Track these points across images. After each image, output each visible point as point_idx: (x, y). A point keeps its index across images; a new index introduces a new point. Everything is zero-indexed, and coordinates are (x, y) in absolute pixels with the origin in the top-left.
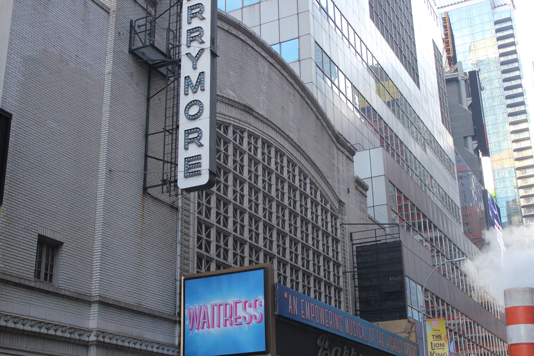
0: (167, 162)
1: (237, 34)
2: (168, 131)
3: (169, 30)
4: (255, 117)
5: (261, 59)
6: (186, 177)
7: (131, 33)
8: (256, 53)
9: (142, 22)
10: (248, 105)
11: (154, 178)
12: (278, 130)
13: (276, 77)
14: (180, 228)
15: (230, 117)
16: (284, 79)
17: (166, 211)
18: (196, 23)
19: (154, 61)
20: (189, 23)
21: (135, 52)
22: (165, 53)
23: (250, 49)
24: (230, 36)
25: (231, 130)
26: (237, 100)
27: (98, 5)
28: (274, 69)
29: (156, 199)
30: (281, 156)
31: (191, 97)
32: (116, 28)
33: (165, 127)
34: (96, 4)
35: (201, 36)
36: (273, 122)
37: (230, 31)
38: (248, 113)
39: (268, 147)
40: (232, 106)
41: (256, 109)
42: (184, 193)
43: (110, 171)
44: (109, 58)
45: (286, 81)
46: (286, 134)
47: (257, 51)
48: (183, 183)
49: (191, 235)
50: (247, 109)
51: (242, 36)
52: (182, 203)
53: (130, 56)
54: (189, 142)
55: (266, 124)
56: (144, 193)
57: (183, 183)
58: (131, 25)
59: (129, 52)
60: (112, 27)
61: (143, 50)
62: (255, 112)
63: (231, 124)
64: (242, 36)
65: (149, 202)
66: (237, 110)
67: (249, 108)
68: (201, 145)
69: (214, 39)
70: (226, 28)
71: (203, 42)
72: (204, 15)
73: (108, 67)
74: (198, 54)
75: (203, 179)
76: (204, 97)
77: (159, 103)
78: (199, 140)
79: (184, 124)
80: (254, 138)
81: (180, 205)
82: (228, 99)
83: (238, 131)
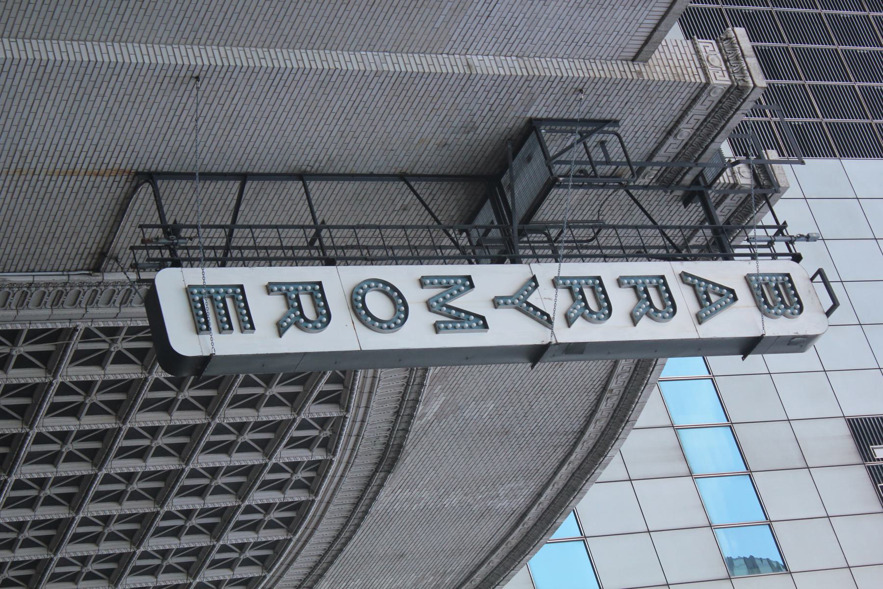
0: (230, 236)
1: (598, 415)
2: (317, 235)
3: (598, 226)
4: (371, 478)
5: (534, 486)
6: (189, 291)
7: (583, 122)
8: (550, 472)
9: (615, 151)
10: (402, 456)
11: (181, 204)
12: (337, 546)
13: (487, 532)
14: (41, 279)
15: (367, 408)
16: (482, 556)
17: (90, 238)
18: (622, 300)
19: (511, 188)
20: (620, 282)
21: (533, 136)
23: (560, 454)
24: (593, 397)
25: (330, 411)
26: (416, 424)
27: (655, 30)
28: (508, 525)
30: (262, 559)
31: (415, 297)
32: (595, 81)
33: (328, 227)
34: (658, 25)
35: (588, 315)
36: (359, 532)
37: (607, 395)
38: (381, 459)
39: (287, 521)
40: (397, 413)
41: (393, 481)
42: (145, 287)
43: (197, 78)
44: (510, 66)
45: (477, 561)
46: (326, 570)
47: (555, 474)
48: (171, 284)
49: (22, 313)
50: (390, 454)
51: (593, 431)
52: (115, 283)
53: (521, 123)
54: (289, 294)
55: (353, 512)
56: (137, 173)
57: (171, 284)
58: (606, 122)
59: (531, 120)
60: (597, 70)
61: (538, 158)
62: (384, 479)
63: (347, 411)
64: (593, 431)
66: (387, 426)
67: (395, 461)
68: (281, 329)
69: (581, 352)
70: (613, 385)
72: (644, 321)
73: (486, 64)
74: (536, 309)
75: (185, 341)
76: (418, 333)
77: (394, 205)
78: (297, 324)
79: (338, 281)
80: (310, 479)
81: (110, 277)
82: (416, 401)
83: (327, 433)
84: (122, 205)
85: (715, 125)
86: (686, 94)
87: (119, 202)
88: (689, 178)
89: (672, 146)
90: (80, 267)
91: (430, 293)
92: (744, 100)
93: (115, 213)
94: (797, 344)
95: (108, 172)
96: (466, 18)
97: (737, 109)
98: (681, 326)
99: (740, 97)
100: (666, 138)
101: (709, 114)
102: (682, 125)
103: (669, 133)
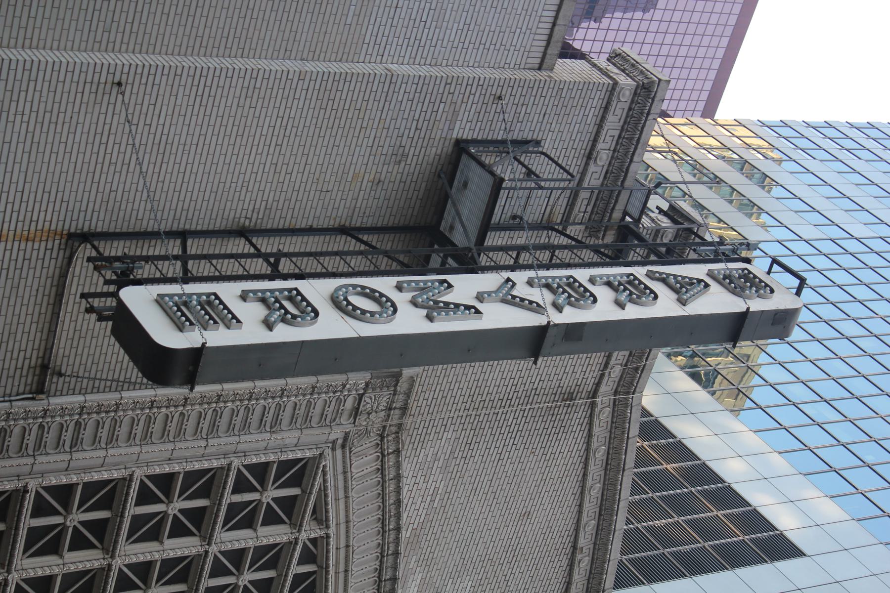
0: (185, 270)
17: (26, 344)
21: (464, 158)
22: (492, 222)
24: (565, 562)
27: (554, 24)
29: (59, 296)
34: (556, 18)
37: (579, 556)
43: (119, 84)
48: (139, 300)
53: (449, 148)
56: (71, 236)
58: (526, 142)
60: (508, 74)
65: (43, 261)
69: (580, 339)
70: (582, 542)
71: (559, 308)
74: (522, 300)
78: (283, 320)
81: (56, 401)
84: (58, 286)
85: (631, 139)
86: (596, 101)
87: (55, 283)
88: (617, 215)
89: (594, 177)
90: (21, 390)
91: (409, 296)
92: (653, 100)
93: (52, 301)
94: (780, 323)
95: (39, 233)
96: (376, 8)
97: (648, 114)
98: (665, 306)
99: (648, 97)
100: (587, 164)
101: (623, 127)
102: (600, 146)
103: (589, 157)
